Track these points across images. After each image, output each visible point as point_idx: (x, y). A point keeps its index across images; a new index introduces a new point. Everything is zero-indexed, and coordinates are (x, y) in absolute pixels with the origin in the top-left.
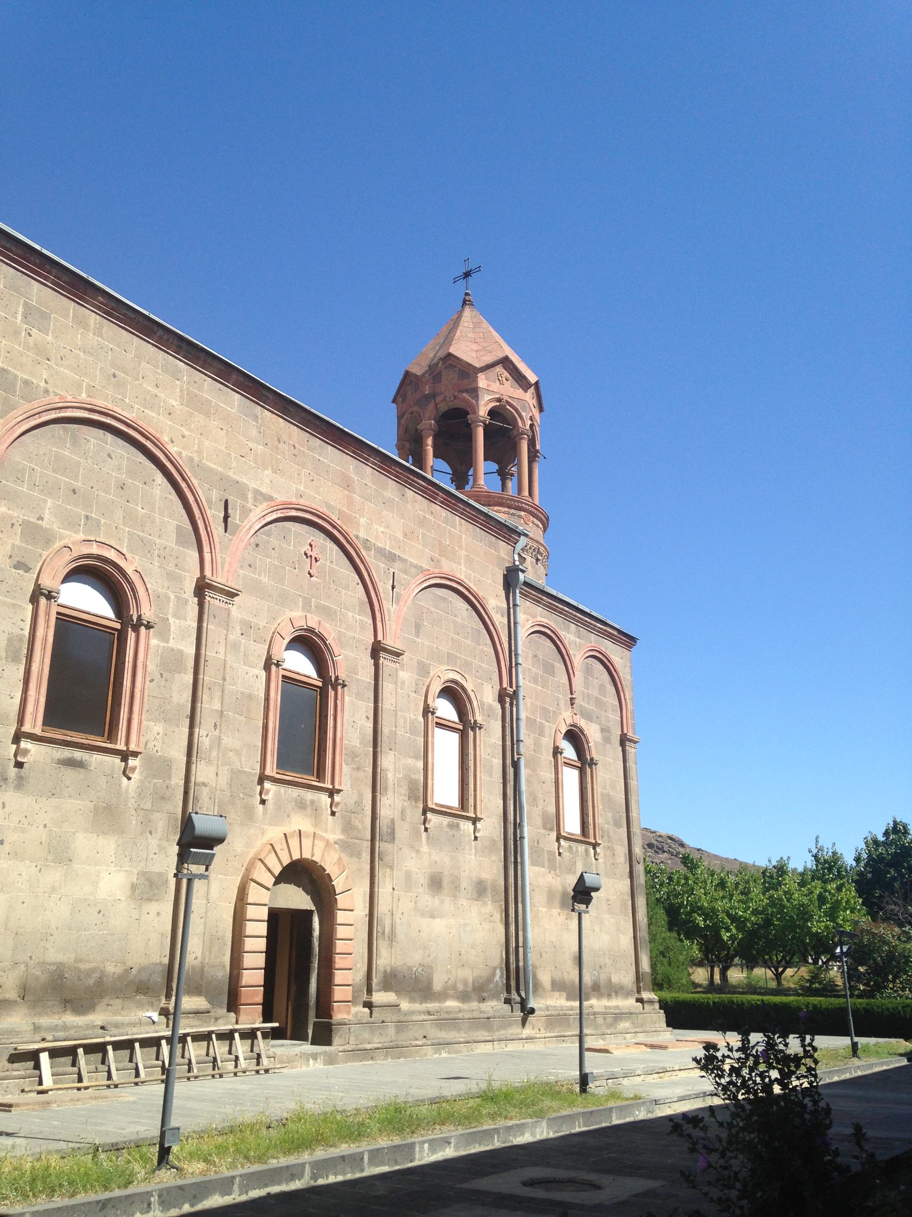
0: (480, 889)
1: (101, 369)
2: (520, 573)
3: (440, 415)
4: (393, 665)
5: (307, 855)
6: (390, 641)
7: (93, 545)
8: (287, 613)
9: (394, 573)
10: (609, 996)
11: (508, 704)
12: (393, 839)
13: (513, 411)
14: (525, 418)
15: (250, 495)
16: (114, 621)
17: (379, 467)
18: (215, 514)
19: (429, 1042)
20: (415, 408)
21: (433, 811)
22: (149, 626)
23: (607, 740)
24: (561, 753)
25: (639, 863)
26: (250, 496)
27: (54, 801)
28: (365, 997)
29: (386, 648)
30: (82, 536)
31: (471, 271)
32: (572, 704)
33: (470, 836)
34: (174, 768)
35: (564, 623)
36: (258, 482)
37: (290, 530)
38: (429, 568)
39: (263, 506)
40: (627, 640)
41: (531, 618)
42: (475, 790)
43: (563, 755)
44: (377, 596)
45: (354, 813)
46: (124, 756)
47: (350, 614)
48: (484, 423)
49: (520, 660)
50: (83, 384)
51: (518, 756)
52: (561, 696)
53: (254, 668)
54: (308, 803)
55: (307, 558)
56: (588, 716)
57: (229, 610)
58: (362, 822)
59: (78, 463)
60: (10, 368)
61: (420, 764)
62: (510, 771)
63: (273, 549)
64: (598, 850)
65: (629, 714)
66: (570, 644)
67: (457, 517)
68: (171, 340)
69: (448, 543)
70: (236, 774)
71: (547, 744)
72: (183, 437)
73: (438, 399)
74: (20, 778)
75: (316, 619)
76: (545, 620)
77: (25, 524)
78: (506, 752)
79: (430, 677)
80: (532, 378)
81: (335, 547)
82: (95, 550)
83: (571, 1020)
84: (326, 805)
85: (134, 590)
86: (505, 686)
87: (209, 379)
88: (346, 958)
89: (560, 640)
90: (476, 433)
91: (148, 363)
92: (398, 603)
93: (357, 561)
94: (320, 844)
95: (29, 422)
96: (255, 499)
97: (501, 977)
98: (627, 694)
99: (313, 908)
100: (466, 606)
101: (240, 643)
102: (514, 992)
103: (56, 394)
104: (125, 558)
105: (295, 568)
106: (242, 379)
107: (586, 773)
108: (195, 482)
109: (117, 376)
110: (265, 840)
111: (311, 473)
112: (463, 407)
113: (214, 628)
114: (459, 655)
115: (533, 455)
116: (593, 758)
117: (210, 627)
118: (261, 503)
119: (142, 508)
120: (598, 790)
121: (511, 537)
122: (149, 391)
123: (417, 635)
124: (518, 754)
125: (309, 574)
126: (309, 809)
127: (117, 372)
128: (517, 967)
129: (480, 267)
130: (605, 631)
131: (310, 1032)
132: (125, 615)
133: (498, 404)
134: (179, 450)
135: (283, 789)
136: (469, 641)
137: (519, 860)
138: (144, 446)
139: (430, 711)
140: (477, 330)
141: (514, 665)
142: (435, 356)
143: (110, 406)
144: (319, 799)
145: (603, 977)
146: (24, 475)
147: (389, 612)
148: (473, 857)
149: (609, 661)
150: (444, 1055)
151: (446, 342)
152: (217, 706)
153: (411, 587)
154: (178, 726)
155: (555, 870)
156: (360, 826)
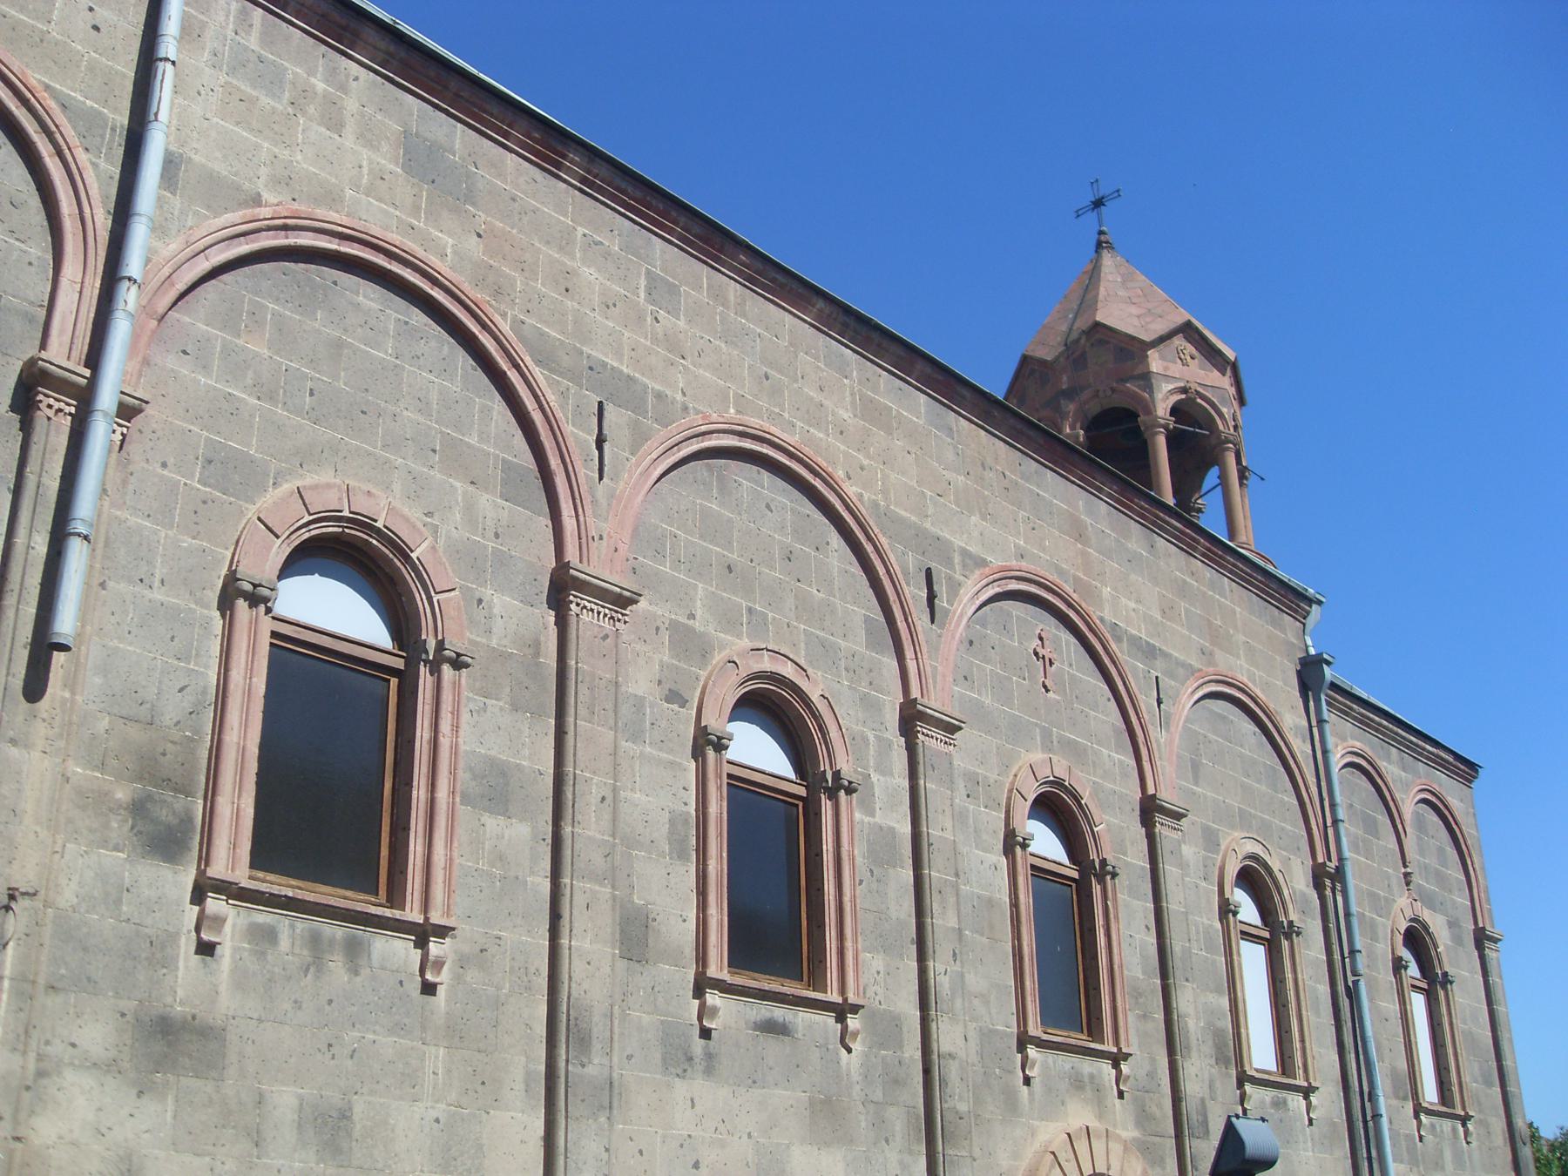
2: (1324, 665)
6: (1168, 795)
7: (763, 654)
8: (1022, 755)
9: (1157, 678)
11: (1329, 889)
15: (957, 559)
16: (792, 782)
18: (915, 593)
22: (850, 791)
23: (1457, 940)
25: (1525, 1144)
26: (956, 561)
27: (757, 1092)
29: (1162, 807)
30: (746, 643)
32: (1408, 884)
34: (905, 1029)
35: (1382, 748)
37: (1009, 615)
38: (1201, 667)
39: (975, 576)
40: (1466, 770)
41: (1339, 742)
42: (1303, 1041)
44: (1139, 719)
45: (1147, 1092)
46: (841, 1012)
49: (1341, 814)
50: (729, 393)
51: (1356, 978)
53: (990, 853)
55: (1038, 660)
56: (1429, 901)
57: (949, 755)
58: (1160, 1106)
59: (730, 520)
60: (637, 375)
61: (1225, 1002)
62: (1345, 1003)
63: (993, 648)
64: (1470, 1126)
65: (1482, 895)
66: (1394, 781)
68: (834, 316)
70: (987, 1035)
71: (1383, 951)
72: (862, 468)
74: (709, 1056)
75: (1065, 763)
76: (1358, 744)
77: (674, 626)
78: (1335, 972)
80: (1230, 354)
81: (1073, 640)
82: (766, 664)
84: (1110, 1080)
85: (822, 729)
86: (1320, 860)
90: (1154, 444)
91: (806, 354)
93: (1106, 661)
94: (1116, 1148)
95: (666, 459)
96: (964, 566)
100: (1252, 727)
101: (968, 811)
103: (698, 412)
104: (807, 675)
105: (1024, 679)
106: (929, 370)
107: (1437, 999)
108: (884, 541)
109: (770, 377)
110: (1037, 1145)
111: (1031, 517)
112: (1127, 406)
113: (934, 786)
114: (1253, 811)
115: (1243, 473)
117: (928, 784)
118: (972, 572)
119: (818, 590)
121: (1298, 606)
122: (812, 398)
123: (1196, 784)
124: (1355, 973)
125: (1045, 686)
127: (769, 371)
129: (1118, 191)
130: (1438, 756)
132: (810, 771)
133: (1183, 396)
134: (860, 491)
136: (1264, 788)
137: (1374, 1153)
139: (1231, 911)
140: (1130, 285)
142: (1071, 329)
143: (767, 426)
144: (1100, 1072)
146: (664, 545)
147: (1159, 746)
148: (1311, 1154)
152: (952, 922)
153: (1184, 699)
154: (901, 957)
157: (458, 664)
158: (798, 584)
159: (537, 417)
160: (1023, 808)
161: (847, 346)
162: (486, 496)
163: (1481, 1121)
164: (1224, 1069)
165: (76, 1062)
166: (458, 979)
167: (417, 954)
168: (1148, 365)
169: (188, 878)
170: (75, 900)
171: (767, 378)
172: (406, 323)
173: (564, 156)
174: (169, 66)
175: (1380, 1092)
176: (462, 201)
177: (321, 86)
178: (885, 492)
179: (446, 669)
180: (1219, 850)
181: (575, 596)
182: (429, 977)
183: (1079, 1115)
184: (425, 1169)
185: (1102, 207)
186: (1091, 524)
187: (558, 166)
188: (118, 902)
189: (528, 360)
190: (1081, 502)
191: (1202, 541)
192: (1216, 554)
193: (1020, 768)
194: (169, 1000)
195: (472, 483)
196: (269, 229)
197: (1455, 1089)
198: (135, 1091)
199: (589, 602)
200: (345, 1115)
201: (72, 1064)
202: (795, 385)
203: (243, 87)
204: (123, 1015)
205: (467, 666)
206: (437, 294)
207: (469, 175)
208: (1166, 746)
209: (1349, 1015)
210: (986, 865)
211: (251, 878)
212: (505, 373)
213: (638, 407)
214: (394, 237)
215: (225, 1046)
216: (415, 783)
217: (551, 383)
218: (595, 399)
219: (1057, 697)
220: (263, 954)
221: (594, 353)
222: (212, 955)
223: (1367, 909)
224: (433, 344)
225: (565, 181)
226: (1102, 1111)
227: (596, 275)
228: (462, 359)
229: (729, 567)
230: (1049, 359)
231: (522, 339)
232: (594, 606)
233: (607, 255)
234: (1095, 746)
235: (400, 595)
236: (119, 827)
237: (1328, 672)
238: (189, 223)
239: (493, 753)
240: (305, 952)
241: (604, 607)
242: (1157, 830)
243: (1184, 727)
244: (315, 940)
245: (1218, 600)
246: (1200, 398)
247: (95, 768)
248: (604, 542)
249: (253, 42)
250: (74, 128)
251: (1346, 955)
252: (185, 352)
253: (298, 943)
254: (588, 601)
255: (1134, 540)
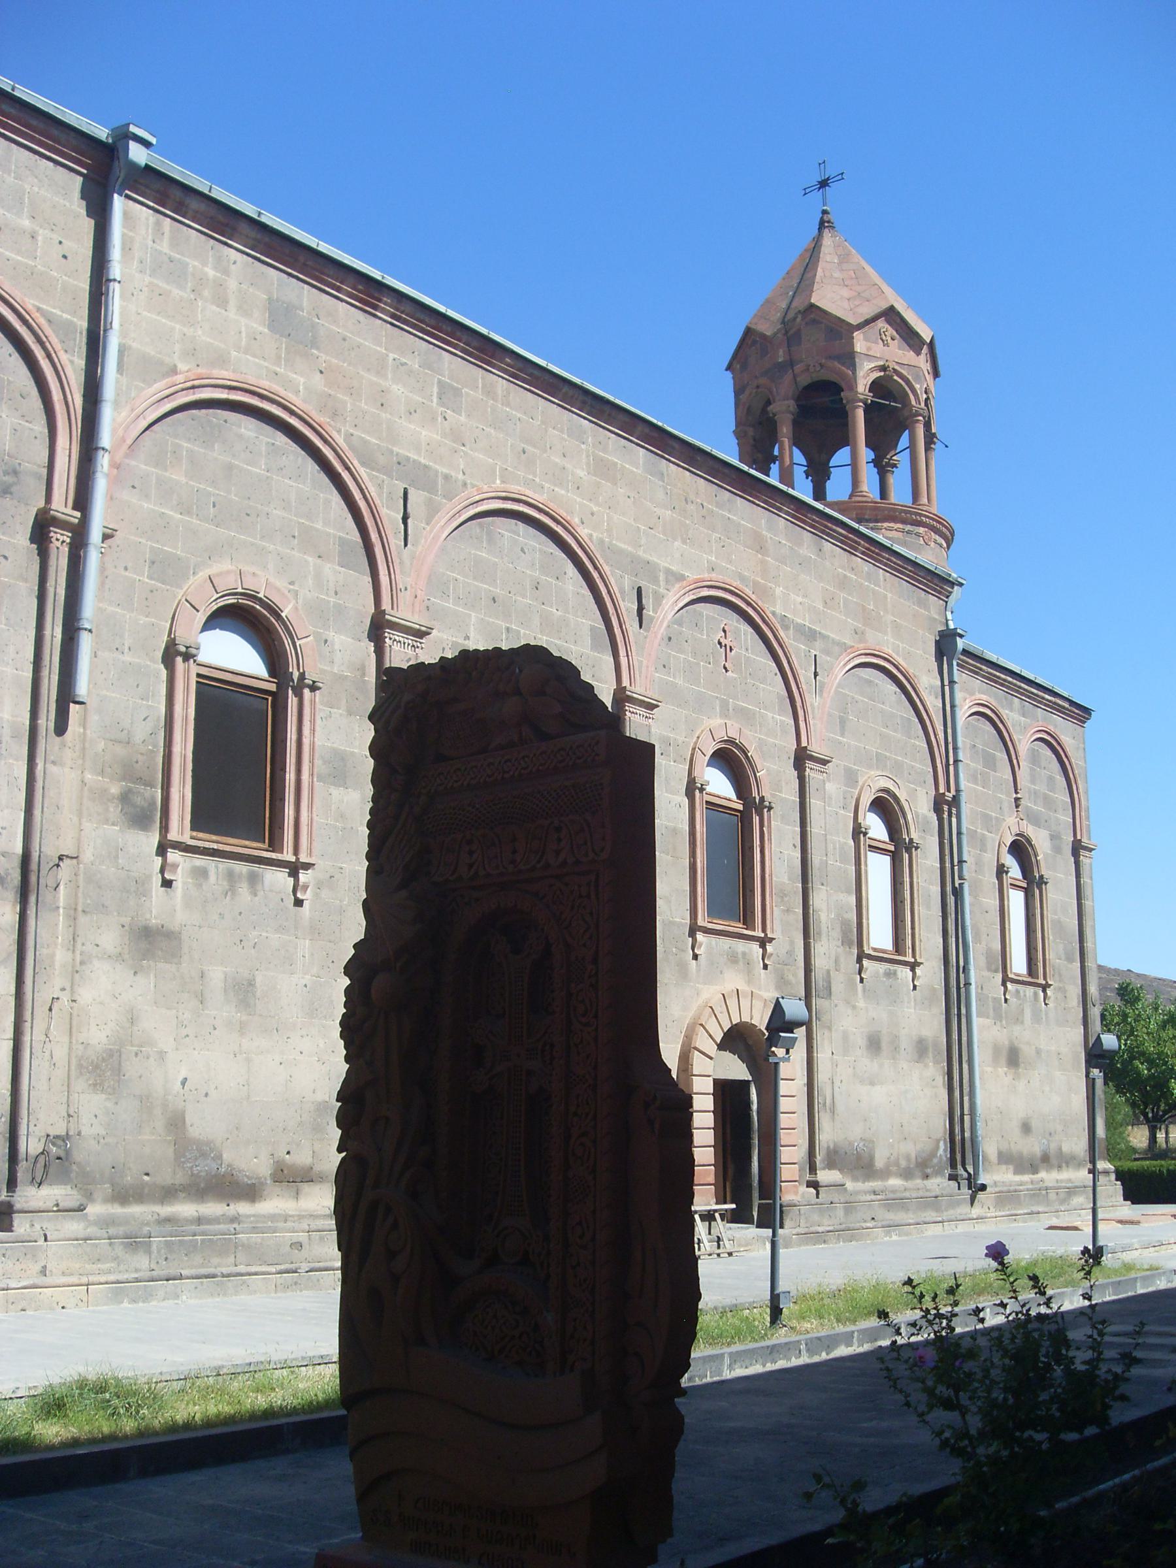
0: (921, 1049)
1: (511, 446)
2: (958, 638)
3: (800, 389)
4: (820, 777)
5: (746, 1018)
6: (816, 748)
9: (815, 656)
10: (1060, 1167)
11: (946, 813)
12: (830, 994)
13: (903, 383)
14: (919, 392)
15: (662, 577)
17: (794, 517)
18: (628, 606)
19: (880, 1225)
20: (763, 381)
21: (870, 957)
23: (1057, 850)
24: (1007, 872)
26: (661, 578)
28: (808, 1177)
29: (812, 756)
31: (828, 179)
32: (1017, 806)
33: (908, 986)
35: (1006, 699)
36: (669, 559)
37: (701, 614)
38: (853, 644)
40: (1081, 713)
41: (968, 696)
42: (913, 928)
43: (1009, 874)
44: (798, 688)
45: (786, 965)
47: (770, 715)
48: (865, 404)
49: (961, 757)
52: (1003, 797)
53: (676, 795)
54: (740, 956)
55: (721, 647)
56: (1035, 820)
58: (795, 975)
59: (495, 564)
60: (431, 464)
61: (852, 900)
62: (951, 900)
65: (1083, 814)
66: (1013, 726)
67: (881, 570)
69: (872, 608)
72: (592, 514)
73: (798, 368)
75: (737, 726)
76: (984, 697)
79: (859, 787)
80: (926, 334)
81: (750, 630)
83: (1022, 1198)
84: (758, 957)
86: (942, 790)
87: (613, 435)
88: (789, 1134)
89: (1002, 722)
90: (854, 417)
91: (554, 428)
92: (821, 696)
96: (667, 581)
97: (945, 1150)
98: (1080, 786)
99: (750, 1079)
100: (895, 688)
102: (959, 1167)
103: (473, 486)
105: (710, 663)
106: (647, 430)
107: (1033, 895)
108: (606, 569)
110: (700, 1001)
112: (832, 379)
115: (930, 439)
116: (1042, 875)
118: (673, 585)
119: (557, 610)
120: (1049, 916)
123: (842, 735)
124: (961, 878)
125: (725, 668)
126: (741, 963)
127: (525, 446)
128: (963, 1139)
129: (842, 174)
130: (1055, 703)
131: (755, 1214)
133: (882, 374)
134: (590, 532)
135: (714, 940)
136: (899, 735)
137: (963, 1011)
138: (556, 532)
139: (862, 832)
140: (845, 266)
141: (951, 762)
145: (1053, 1146)
146: (448, 588)
147: (813, 708)
148: (913, 1011)
149: (1059, 744)
150: (894, 1238)
151: (803, 284)
153: (837, 671)
155: (1001, 1021)
156: (794, 982)
157: (314, 688)
158: (543, 607)
159: (362, 504)
160: (702, 760)
161: (585, 418)
162: (329, 565)
163: (1060, 988)
164: (848, 949)
165: (100, 955)
166: (316, 895)
167: (291, 881)
168: (852, 345)
169: (155, 839)
170: (92, 858)
171: (524, 453)
172: (273, 444)
173: (380, 300)
174: (117, 284)
175: (972, 967)
176: (309, 346)
177: (211, 272)
178: (609, 531)
179: (306, 691)
180: (857, 786)
181: (389, 633)
182: (299, 895)
183: (733, 980)
184: (299, 1016)
185: (827, 188)
186: (771, 538)
187: (375, 307)
188: (117, 857)
189: (356, 463)
190: (763, 521)
191: (862, 542)
192: (873, 552)
193: (702, 731)
194: (148, 916)
195: (319, 557)
196: (183, 390)
197: (1040, 965)
198: (133, 972)
199: (398, 636)
200: (251, 984)
201: (97, 956)
202: (545, 455)
203: (160, 284)
204: (123, 926)
205: (319, 688)
206: (293, 421)
207: (313, 326)
208: (819, 709)
209: (953, 909)
210: (673, 804)
211: (192, 838)
212: (340, 474)
213: (431, 488)
214: (265, 384)
215: (180, 943)
216: (288, 770)
217: (372, 478)
218: (401, 486)
219: (734, 675)
220: (201, 885)
221: (401, 451)
222: (170, 887)
223: (980, 827)
224: (291, 457)
225: (380, 318)
226: (750, 977)
227: (402, 390)
228: (311, 466)
229: (494, 599)
230: (768, 333)
231: (351, 448)
232: (401, 639)
233: (410, 372)
234: (762, 711)
235: (273, 641)
236: (114, 810)
237: (960, 644)
238: (133, 395)
239: (335, 745)
240: (225, 883)
241: (407, 639)
242: (807, 774)
243: (836, 692)
244: (230, 875)
245: (873, 590)
246: (897, 376)
247: (98, 774)
248: (408, 592)
249: (164, 247)
250: (57, 336)
251: (956, 863)
252: (133, 487)
253: (220, 877)
254: (398, 636)
255: (805, 546)
